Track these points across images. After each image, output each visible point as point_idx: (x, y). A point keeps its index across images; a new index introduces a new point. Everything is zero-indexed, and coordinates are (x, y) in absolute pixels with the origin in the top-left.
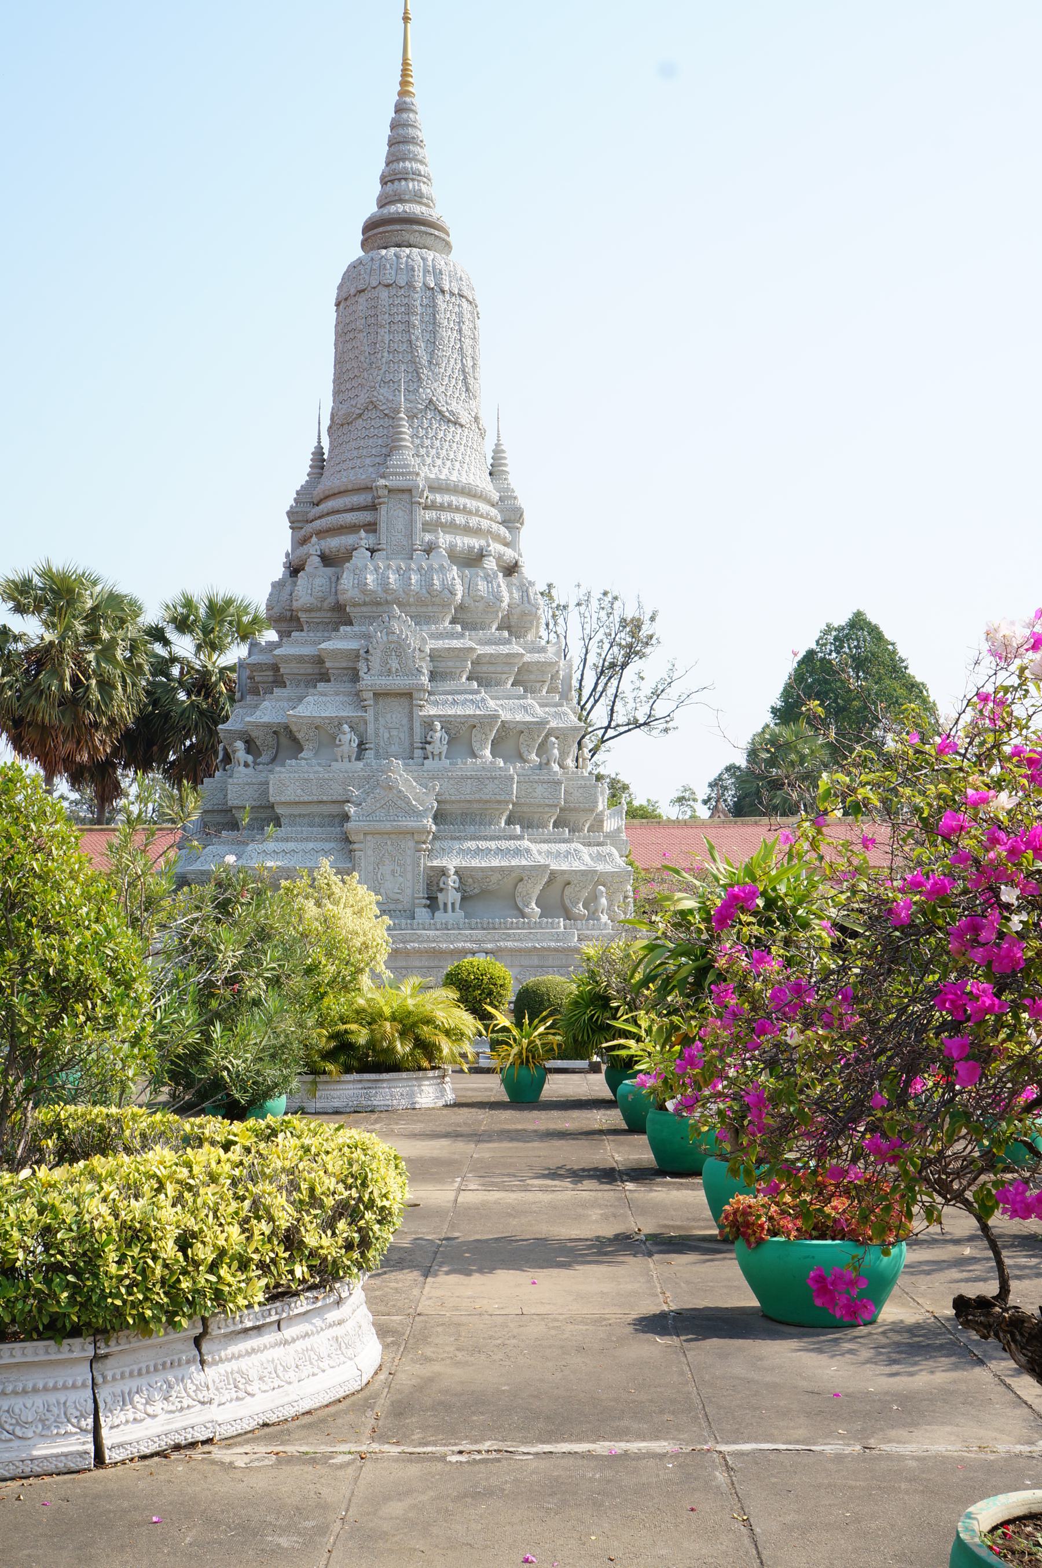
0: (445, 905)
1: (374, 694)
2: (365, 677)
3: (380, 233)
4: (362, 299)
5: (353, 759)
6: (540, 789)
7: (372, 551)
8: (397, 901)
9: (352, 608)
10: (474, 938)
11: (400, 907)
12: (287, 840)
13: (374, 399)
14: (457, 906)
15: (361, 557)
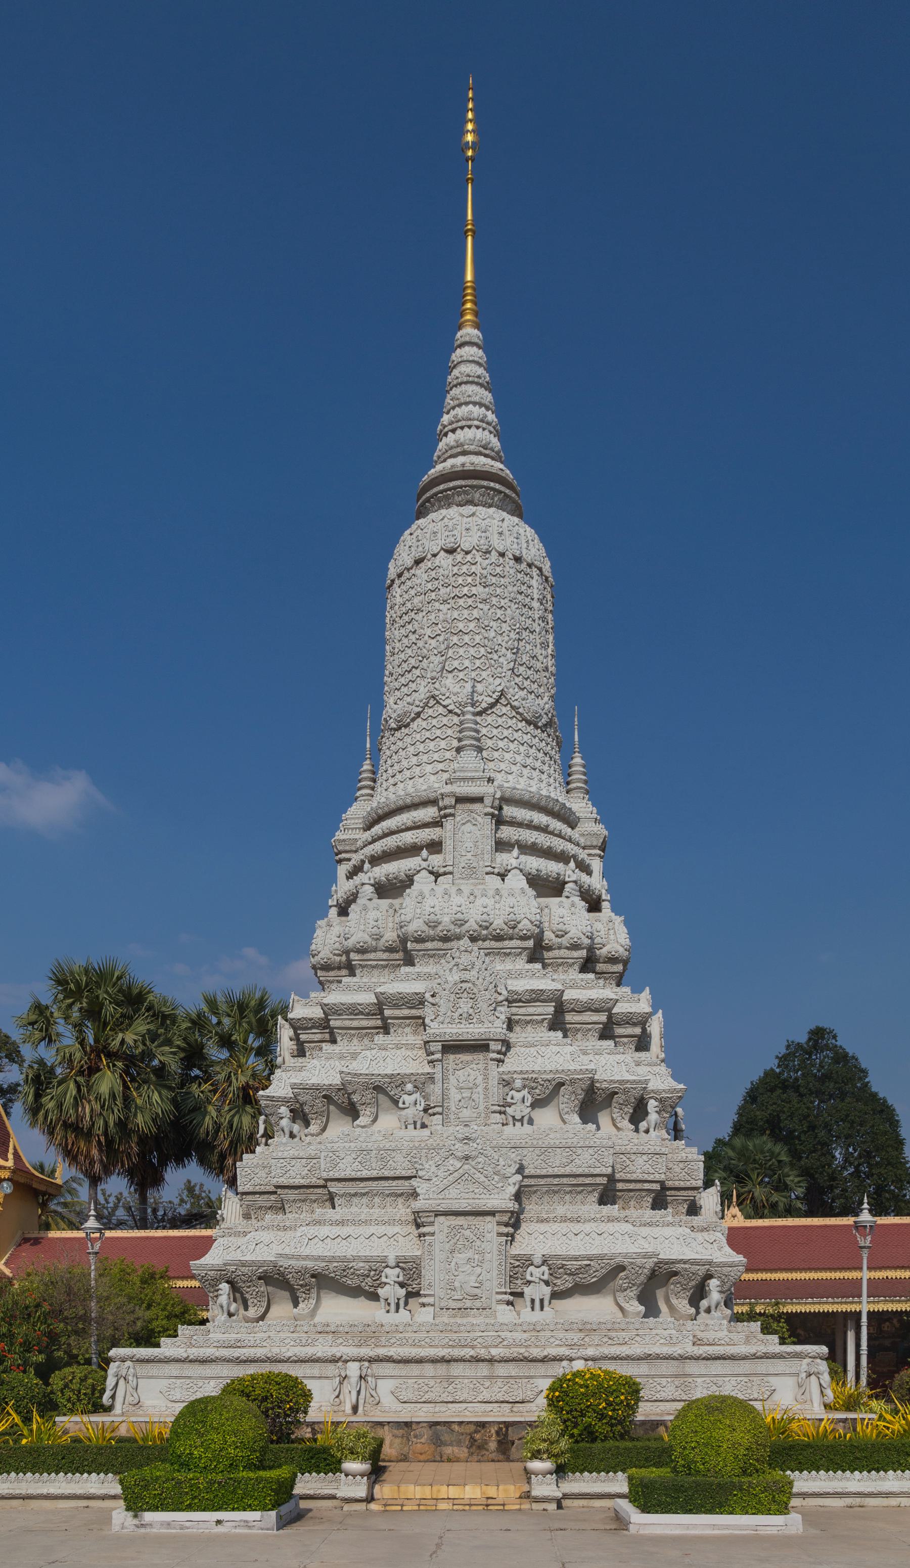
0: (533, 1301)
1: (443, 1045)
2: (432, 1024)
3: (441, 492)
4: (419, 571)
5: (418, 1126)
6: (640, 1160)
7: (437, 875)
8: (475, 1297)
9: (415, 944)
10: (569, 1342)
11: (478, 1304)
12: (342, 1223)
13: (437, 693)
14: (546, 1303)
15: (423, 881)
